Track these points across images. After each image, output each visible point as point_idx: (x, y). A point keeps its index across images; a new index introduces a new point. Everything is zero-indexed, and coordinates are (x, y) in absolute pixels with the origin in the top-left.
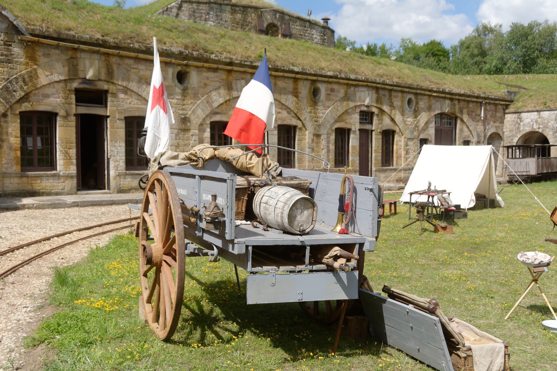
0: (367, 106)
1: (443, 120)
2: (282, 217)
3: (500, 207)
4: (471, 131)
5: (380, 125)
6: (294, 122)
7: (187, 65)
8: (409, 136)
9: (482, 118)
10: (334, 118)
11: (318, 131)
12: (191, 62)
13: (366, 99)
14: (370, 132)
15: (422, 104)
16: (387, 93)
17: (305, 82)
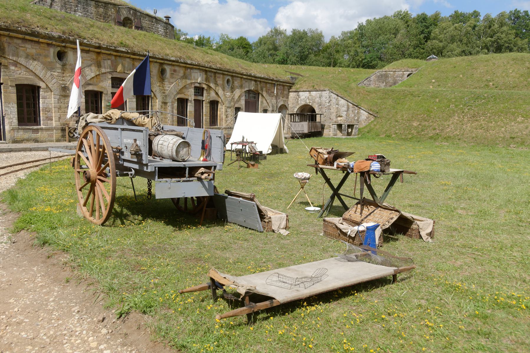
0: (199, 83)
2: (172, 152)
3: (286, 153)
7: (65, 47)
12: (68, 45)
13: (199, 78)
15: (237, 83)
16: (213, 75)
17: (155, 64)
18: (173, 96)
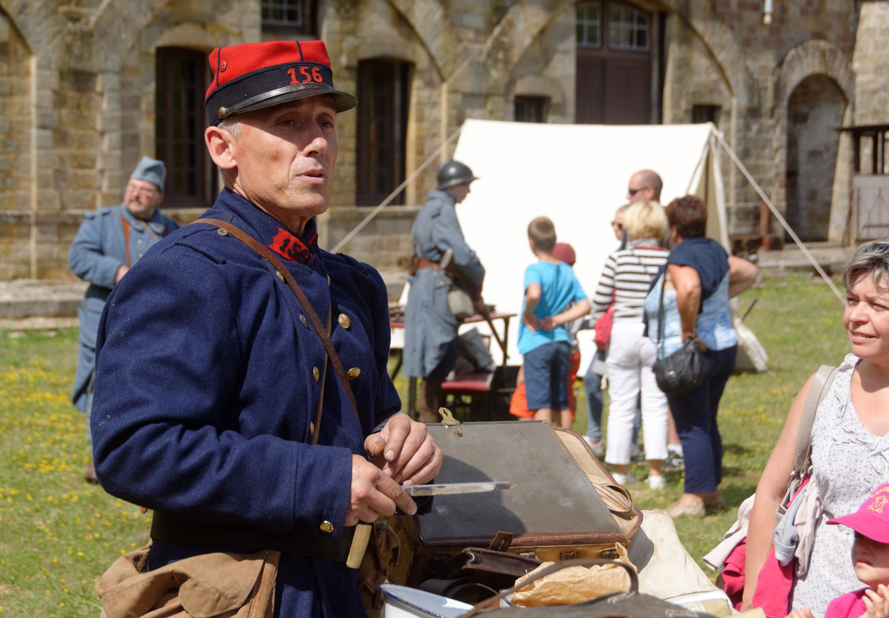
1: (612, 25)
3: (753, 371)
4: (721, 69)
5: (351, 41)
8: (468, 85)
9: (768, 19)
10: (151, 8)
11: (80, 58)
18: (127, 38)
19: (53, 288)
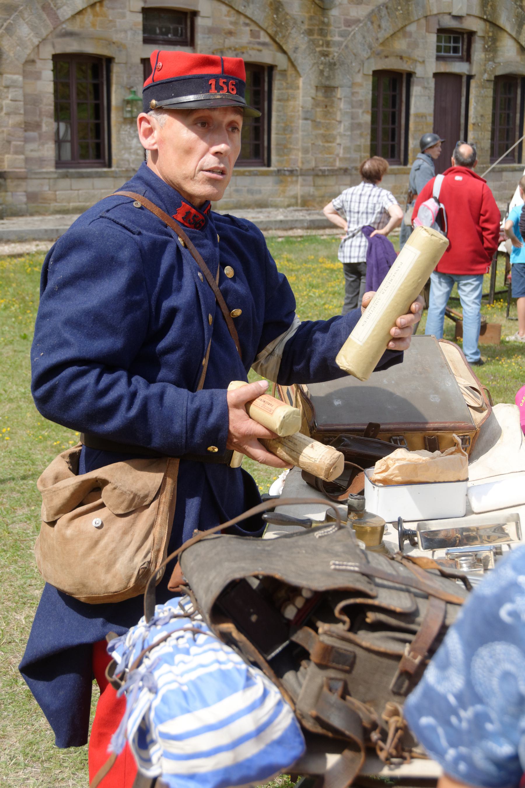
0: (458, 18)
6: (267, 56)
10: (370, 48)
11: (328, 78)
14: (464, 80)
19: (309, 212)
